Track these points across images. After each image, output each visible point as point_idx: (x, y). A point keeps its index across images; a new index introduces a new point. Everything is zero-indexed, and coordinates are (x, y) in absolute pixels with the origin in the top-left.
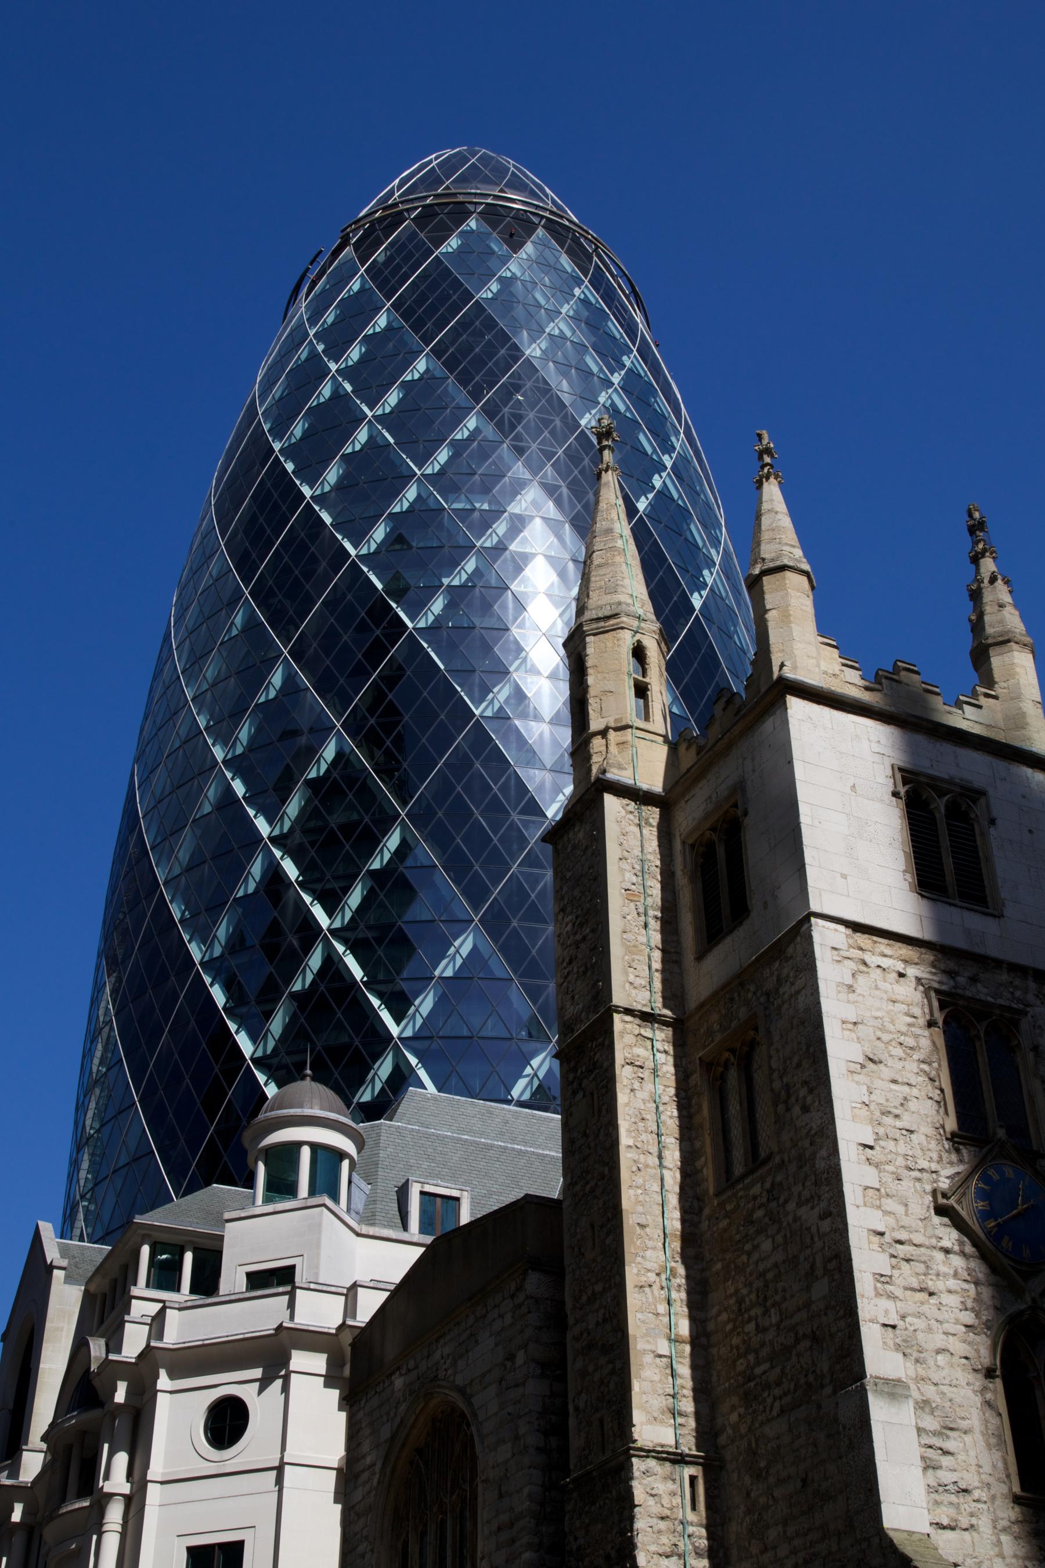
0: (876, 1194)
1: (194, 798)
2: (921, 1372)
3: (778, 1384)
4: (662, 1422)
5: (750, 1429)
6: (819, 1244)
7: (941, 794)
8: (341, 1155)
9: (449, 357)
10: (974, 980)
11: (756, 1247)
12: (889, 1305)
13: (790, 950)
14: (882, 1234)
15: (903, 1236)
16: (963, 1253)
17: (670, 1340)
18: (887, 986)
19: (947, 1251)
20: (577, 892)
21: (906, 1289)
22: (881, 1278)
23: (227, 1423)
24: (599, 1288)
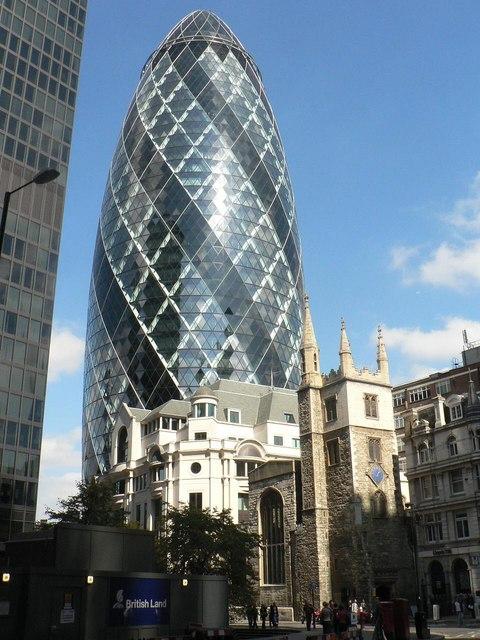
1: (126, 247)
9: (203, 102)
23: (196, 468)
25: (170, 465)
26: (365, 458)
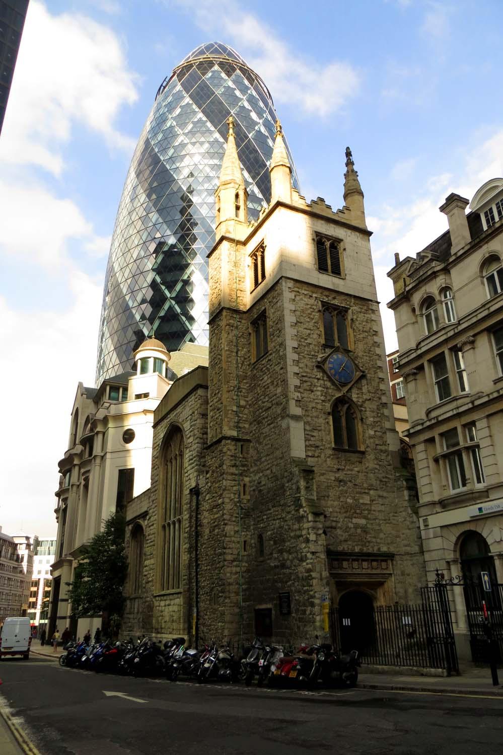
0: (297, 362)
2: (307, 414)
3: (267, 417)
4: (234, 430)
5: (259, 431)
6: (279, 377)
7: (329, 240)
8: (163, 361)
10: (334, 298)
11: (263, 379)
12: (299, 395)
13: (276, 288)
14: (298, 374)
15: (305, 374)
16: (323, 380)
17: (237, 406)
18: (306, 300)
19: (318, 379)
20: (215, 273)
21: (304, 390)
22: (296, 386)
24: (217, 392)
25: (100, 436)
26: (317, 337)
